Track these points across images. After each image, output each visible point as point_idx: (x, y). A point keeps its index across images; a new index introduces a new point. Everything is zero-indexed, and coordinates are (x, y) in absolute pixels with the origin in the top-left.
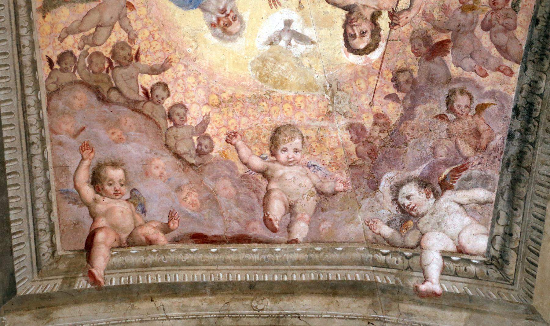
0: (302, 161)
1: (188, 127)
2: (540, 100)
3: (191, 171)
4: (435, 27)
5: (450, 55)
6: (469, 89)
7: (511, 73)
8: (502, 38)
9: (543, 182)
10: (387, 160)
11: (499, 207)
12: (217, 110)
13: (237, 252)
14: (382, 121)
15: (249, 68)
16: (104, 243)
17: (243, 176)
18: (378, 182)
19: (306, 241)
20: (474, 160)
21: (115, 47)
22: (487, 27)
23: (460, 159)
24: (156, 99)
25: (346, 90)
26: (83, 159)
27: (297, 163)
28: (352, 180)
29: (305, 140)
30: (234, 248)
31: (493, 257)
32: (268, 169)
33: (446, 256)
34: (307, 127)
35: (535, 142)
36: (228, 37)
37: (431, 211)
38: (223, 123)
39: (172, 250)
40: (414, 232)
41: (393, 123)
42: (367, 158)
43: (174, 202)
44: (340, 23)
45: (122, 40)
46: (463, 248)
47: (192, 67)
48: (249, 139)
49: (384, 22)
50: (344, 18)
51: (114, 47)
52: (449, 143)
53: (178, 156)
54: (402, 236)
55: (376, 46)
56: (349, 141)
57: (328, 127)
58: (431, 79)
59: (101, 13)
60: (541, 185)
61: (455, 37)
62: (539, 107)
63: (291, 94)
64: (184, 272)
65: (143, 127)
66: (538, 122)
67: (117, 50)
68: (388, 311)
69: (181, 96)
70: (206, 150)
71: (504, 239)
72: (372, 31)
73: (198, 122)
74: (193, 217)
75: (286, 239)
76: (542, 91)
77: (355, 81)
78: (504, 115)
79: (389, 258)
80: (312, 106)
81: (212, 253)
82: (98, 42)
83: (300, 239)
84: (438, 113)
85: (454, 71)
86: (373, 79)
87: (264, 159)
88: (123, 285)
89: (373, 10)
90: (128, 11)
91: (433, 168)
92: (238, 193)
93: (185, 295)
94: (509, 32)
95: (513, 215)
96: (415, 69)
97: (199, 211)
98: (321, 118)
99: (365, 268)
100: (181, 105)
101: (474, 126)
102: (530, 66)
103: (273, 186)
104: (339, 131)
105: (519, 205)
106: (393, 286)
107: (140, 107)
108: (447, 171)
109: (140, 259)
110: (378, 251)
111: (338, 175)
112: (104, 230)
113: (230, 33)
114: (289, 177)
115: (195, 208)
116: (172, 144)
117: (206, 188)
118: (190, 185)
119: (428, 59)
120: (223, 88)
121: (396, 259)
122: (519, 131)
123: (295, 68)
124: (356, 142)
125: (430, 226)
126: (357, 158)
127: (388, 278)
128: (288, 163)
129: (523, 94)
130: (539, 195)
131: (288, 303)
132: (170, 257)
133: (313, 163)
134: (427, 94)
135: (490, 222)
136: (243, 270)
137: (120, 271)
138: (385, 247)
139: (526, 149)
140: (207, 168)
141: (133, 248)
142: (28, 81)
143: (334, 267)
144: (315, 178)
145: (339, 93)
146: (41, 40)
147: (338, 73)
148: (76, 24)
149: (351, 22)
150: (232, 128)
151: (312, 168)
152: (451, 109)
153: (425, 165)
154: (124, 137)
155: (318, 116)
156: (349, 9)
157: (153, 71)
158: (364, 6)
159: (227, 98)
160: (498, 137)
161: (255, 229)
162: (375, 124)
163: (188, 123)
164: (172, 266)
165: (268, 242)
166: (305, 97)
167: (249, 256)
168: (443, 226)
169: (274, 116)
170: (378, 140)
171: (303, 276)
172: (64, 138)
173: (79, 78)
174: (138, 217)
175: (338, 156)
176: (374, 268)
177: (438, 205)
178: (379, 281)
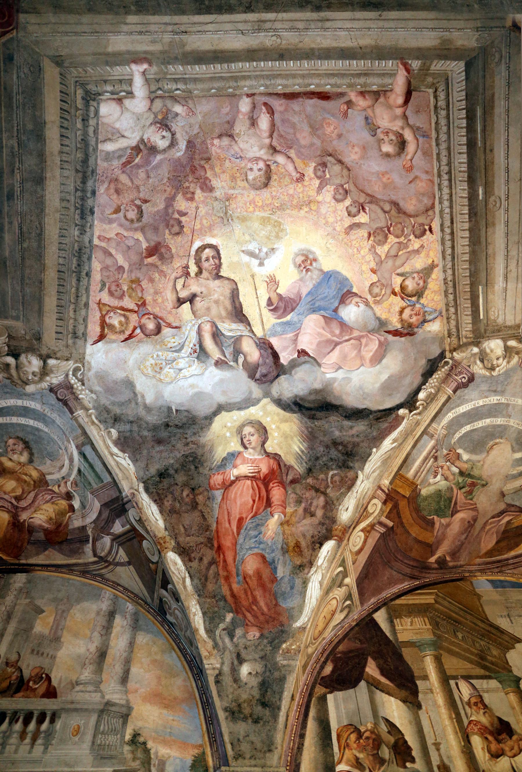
0: (246, 161)
1: (333, 185)
2: (77, 222)
3: (330, 150)
4: (157, 267)
5: (144, 247)
6: (127, 223)
7: (99, 237)
8: (109, 261)
9: (66, 164)
10: (182, 166)
11: (94, 139)
12: (311, 198)
13: (294, 85)
14: (189, 196)
15: (288, 231)
16: (397, 95)
17: (291, 148)
18: (187, 147)
19: (240, 96)
20: (117, 172)
21: (385, 242)
22: (121, 268)
23: (128, 171)
24: (357, 205)
25: (216, 218)
26: (411, 160)
27: (250, 160)
28: (207, 148)
29: (245, 178)
30: (297, 89)
31: (94, 100)
32: (272, 154)
33: (130, 94)
34: (244, 188)
35: (76, 192)
36: (304, 252)
37: (146, 128)
38: (307, 189)
39: (345, 87)
40: (157, 110)
41: (180, 195)
42: (197, 166)
43: (344, 126)
44: (224, 266)
45: (380, 247)
46: (118, 103)
47: (330, 229)
48: (287, 178)
49: (193, 269)
50: (221, 270)
51: (386, 242)
52: (137, 182)
53: (340, 162)
54: (166, 106)
55: (197, 251)
56: (212, 179)
57: (229, 190)
58: (156, 229)
59: (394, 265)
60: (67, 162)
61: (142, 260)
62: (77, 217)
63: (257, 213)
64: (336, 68)
65: (366, 183)
66: (75, 206)
67: (384, 240)
68: (171, 42)
69: (338, 208)
70: (319, 167)
71: (88, 115)
72: (201, 262)
73: (325, 188)
74: (329, 113)
75: (255, 97)
76: (76, 228)
77: (211, 225)
78: (100, 208)
79: (174, 87)
80: (241, 205)
81: (314, 84)
82: (397, 245)
83: (245, 97)
84: (148, 204)
85: (139, 236)
86: (198, 226)
87: (275, 162)
88: (383, 60)
89: (202, 276)
90: (375, 268)
91: (147, 162)
92: (295, 134)
93: (335, 48)
94: (105, 266)
95: (83, 135)
96: (167, 236)
97: (324, 119)
98: (234, 196)
99: (193, 76)
100: (338, 201)
101: (121, 197)
102: (87, 244)
103: (267, 141)
104: (220, 186)
105: (80, 143)
106: (169, 63)
107: (368, 199)
108: (137, 160)
109: (370, 80)
110: (184, 91)
111: (219, 151)
112: (398, 106)
113: (303, 255)
114: (256, 149)
115: (327, 121)
116: (345, 172)
117: (319, 137)
118: (331, 139)
119: (159, 243)
120: (307, 215)
121: (169, 86)
122: (88, 198)
123: (255, 233)
124: (207, 178)
125: (145, 117)
126: (205, 166)
127: (173, 70)
128: (257, 159)
129: (89, 225)
130: (67, 153)
131: (252, 43)
132: (346, 81)
133: (238, 160)
134: (157, 217)
135: (100, 127)
136: (289, 70)
137: (385, 72)
138: (177, 95)
139: (81, 185)
140: (319, 153)
141: (375, 90)
142: (447, 217)
143: (217, 75)
144: (236, 148)
145: (222, 215)
146: (436, 246)
147: (223, 230)
148: (412, 257)
149: (216, 267)
150: (300, 185)
151: (238, 156)
152: (139, 208)
153: (154, 164)
154: (381, 176)
155: (236, 197)
156: (218, 277)
157: (358, 225)
158: (208, 279)
159: (304, 207)
160: (102, 191)
161: (281, 105)
162: (193, 193)
163: (333, 188)
164: (345, 74)
165: (270, 94)
166: (246, 211)
167: (284, 82)
168: (135, 118)
169: (269, 196)
170: (190, 180)
171: (241, 67)
172: (424, 177)
173: (411, 219)
174: (371, 114)
175: (219, 167)
176: (185, 76)
177: (141, 134)
178: (180, 66)
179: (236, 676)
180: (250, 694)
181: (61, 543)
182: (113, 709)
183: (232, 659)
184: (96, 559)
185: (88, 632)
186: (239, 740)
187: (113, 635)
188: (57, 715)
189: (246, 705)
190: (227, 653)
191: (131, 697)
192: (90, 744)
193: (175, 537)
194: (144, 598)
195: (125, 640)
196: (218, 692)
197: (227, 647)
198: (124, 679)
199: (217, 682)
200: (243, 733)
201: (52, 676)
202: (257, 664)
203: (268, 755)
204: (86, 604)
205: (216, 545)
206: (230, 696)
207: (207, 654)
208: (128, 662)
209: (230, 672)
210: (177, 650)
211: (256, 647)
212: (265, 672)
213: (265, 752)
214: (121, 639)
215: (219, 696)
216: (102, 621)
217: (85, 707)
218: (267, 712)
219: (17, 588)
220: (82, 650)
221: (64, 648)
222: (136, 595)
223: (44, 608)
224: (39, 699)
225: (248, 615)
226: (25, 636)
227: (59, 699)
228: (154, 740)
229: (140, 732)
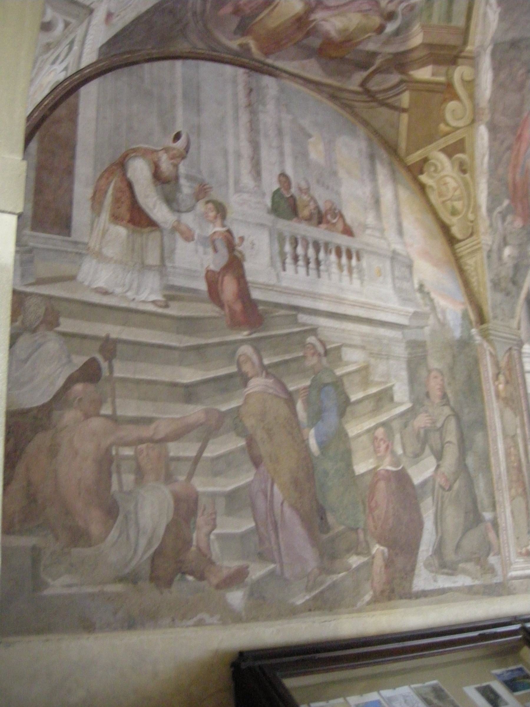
181: (332, 58)
184: (360, 89)
193: (493, 110)
198: (400, 232)
205: (519, 133)
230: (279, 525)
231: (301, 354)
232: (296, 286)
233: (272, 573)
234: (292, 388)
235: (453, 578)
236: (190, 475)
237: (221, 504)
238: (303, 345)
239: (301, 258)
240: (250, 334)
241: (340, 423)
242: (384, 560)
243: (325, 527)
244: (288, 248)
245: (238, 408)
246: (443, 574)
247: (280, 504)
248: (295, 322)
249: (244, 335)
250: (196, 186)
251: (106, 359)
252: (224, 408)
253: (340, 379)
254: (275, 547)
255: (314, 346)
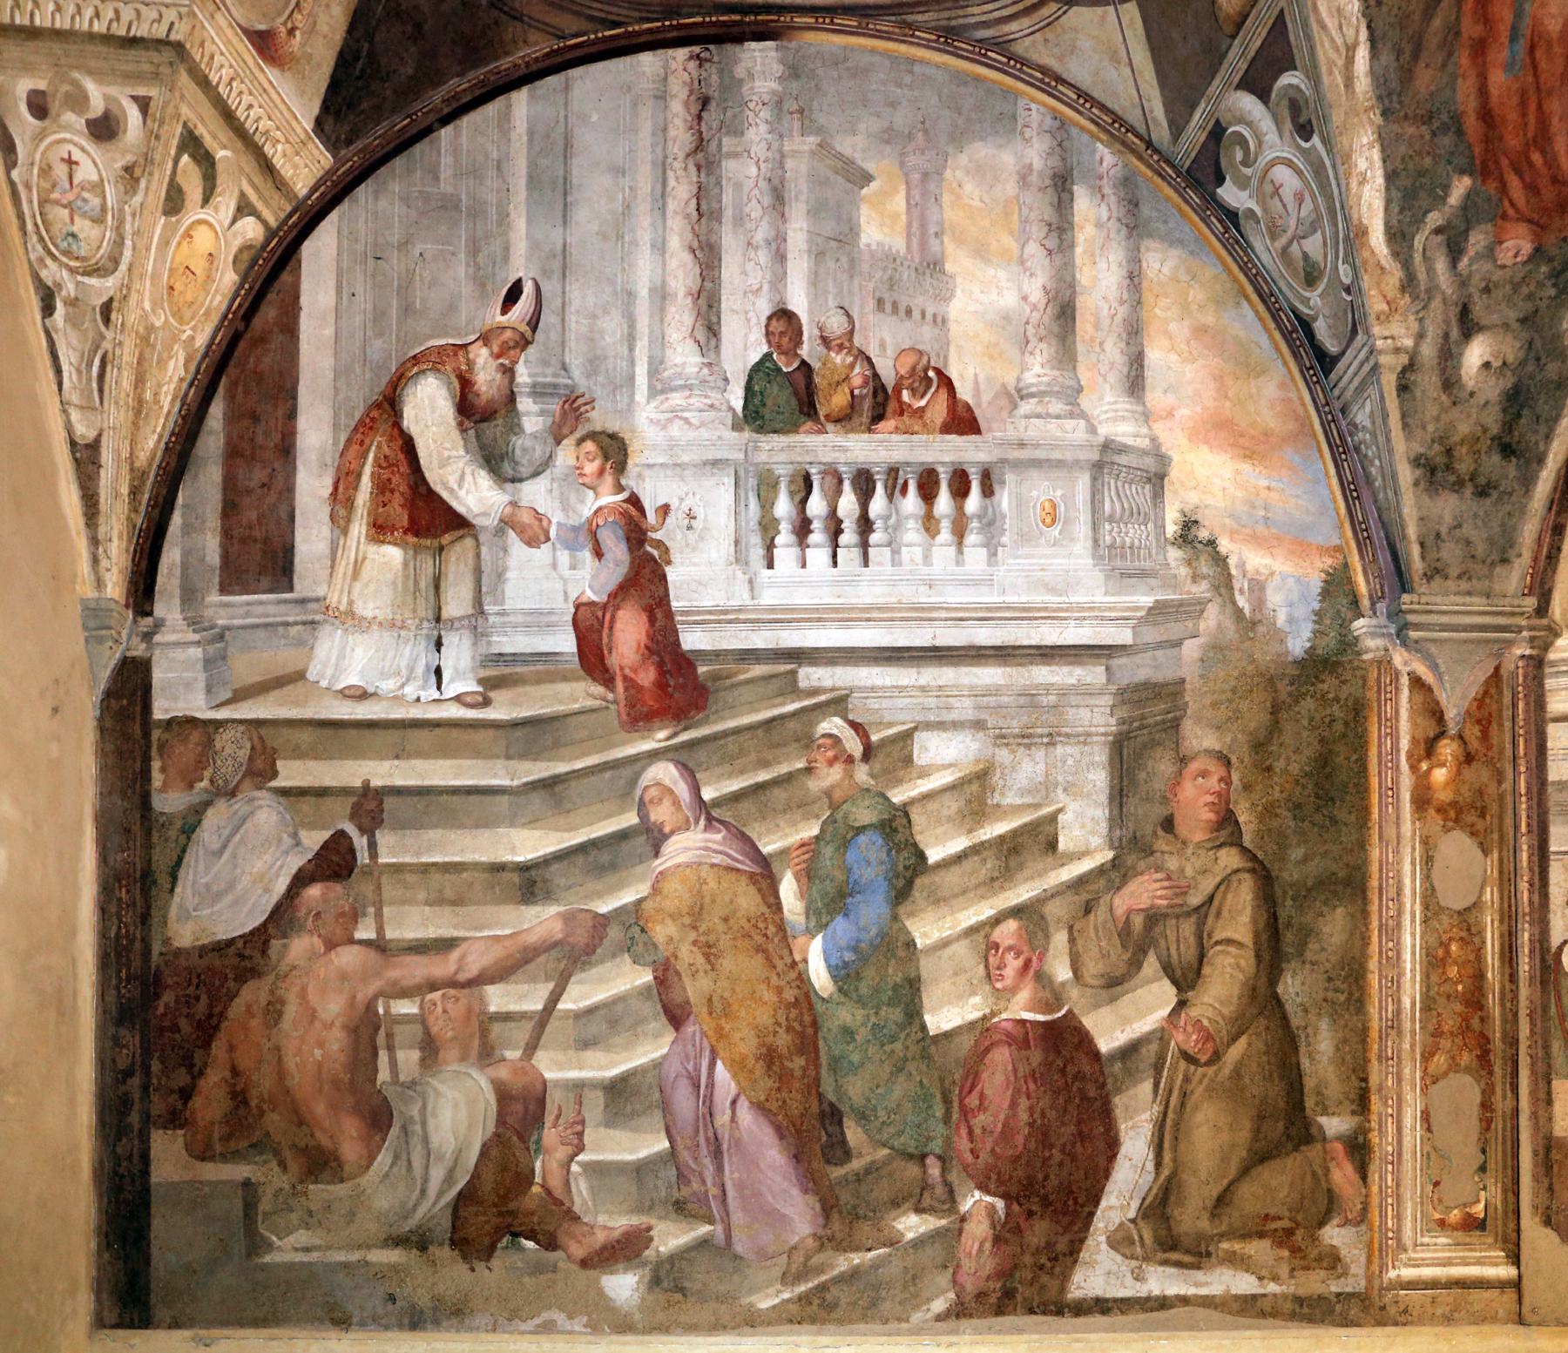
179: (1449, 371)
180: (1478, 423)
182: (1123, 459)
183: (1447, 322)
185: (1009, 242)
186: (1438, 535)
187: (1079, 250)
188: (994, 477)
189: (1464, 451)
190: (1436, 303)
191: (1160, 429)
192: (1089, 544)
194: (1142, 129)
195: (1114, 267)
196: (1403, 416)
197: (1437, 287)
198: (1135, 383)
199: (1403, 388)
200: (1448, 519)
201: (953, 373)
202: (1509, 338)
203: (1498, 570)
204: (981, 150)
206: (1430, 428)
207: (1384, 307)
208: (1134, 332)
209: (1436, 361)
210: (1254, 297)
211: (1516, 288)
212: (1523, 363)
213: (1493, 564)
214: (1103, 265)
215: (1405, 426)
216: (1039, 205)
217: (1056, 455)
218: (1512, 469)
219: (766, 98)
220: (1010, 300)
221: (959, 292)
222: (1117, 118)
223: (870, 166)
224: (939, 437)
225: (1514, 183)
226: (844, 259)
227: (987, 436)
228: (1232, 534)
229: (1199, 517)
230: (725, 1146)
231: (800, 764)
232: (802, 598)
233: (704, 1243)
234: (767, 849)
235: (1199, 1275)
236: (531, 1047)
237: (595, 1104)
238: (807, 741)
239: (816, 525)
240: (675, 734)
241: (895, 918)
242: (993, 1226)
243: (839, 1150)
244: (783, 507)
245: (639, 902)
246: (1165, 1263)
247: (728, 1104)
248: (790, 687)
249: (659, 738)
250: (555, 406)
251: (362, 830)
252: (604, 907)
253: (904, 810)
254: (714, 1191)
255: (836, 740)
